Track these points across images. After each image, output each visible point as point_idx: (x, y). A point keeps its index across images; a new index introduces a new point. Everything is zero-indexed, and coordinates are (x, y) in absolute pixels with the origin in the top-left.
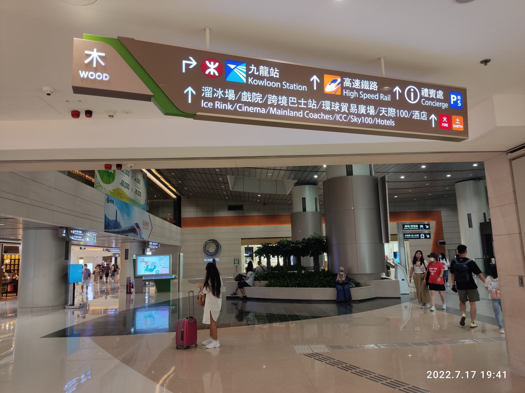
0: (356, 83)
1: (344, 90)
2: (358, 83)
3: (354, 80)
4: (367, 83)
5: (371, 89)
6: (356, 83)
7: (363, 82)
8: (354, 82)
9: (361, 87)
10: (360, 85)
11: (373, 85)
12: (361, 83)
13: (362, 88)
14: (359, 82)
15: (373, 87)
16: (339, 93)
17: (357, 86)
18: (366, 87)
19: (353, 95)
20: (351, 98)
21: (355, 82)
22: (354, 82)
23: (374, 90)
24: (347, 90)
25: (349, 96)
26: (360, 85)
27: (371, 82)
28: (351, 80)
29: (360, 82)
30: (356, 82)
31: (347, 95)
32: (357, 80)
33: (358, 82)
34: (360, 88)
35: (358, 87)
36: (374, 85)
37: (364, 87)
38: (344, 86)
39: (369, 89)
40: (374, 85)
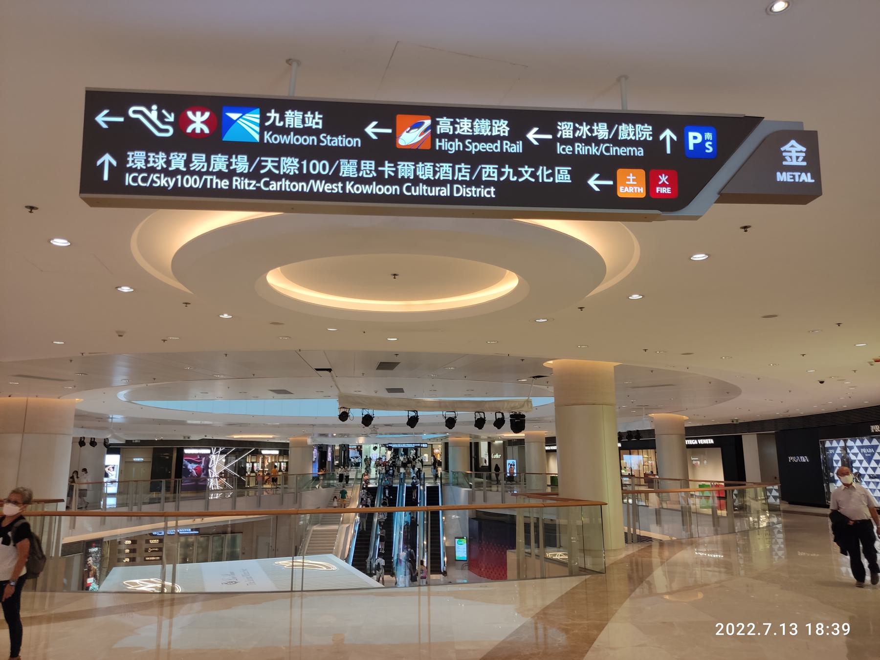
0: (463, 125)
2: (468, 125)
3: (458, 120)
6: (463, 125)
9: (473, 132)
10: (472, 128)
11: (498, 127)
12: (474, 124)
13: (475, 134)
14: (470, 124)
17: (466, 131)
18: (483, 131)
21: (462, 123)
22: (459, 123)
26: (472, 128)
28: (452, 120)
29: (472, 123)
30: (463, 123)
34: (471, 134)
35: (468, 131)
36: (502, 126)
37: (480, 132)
39: (489, 134)
40: (502, 126)
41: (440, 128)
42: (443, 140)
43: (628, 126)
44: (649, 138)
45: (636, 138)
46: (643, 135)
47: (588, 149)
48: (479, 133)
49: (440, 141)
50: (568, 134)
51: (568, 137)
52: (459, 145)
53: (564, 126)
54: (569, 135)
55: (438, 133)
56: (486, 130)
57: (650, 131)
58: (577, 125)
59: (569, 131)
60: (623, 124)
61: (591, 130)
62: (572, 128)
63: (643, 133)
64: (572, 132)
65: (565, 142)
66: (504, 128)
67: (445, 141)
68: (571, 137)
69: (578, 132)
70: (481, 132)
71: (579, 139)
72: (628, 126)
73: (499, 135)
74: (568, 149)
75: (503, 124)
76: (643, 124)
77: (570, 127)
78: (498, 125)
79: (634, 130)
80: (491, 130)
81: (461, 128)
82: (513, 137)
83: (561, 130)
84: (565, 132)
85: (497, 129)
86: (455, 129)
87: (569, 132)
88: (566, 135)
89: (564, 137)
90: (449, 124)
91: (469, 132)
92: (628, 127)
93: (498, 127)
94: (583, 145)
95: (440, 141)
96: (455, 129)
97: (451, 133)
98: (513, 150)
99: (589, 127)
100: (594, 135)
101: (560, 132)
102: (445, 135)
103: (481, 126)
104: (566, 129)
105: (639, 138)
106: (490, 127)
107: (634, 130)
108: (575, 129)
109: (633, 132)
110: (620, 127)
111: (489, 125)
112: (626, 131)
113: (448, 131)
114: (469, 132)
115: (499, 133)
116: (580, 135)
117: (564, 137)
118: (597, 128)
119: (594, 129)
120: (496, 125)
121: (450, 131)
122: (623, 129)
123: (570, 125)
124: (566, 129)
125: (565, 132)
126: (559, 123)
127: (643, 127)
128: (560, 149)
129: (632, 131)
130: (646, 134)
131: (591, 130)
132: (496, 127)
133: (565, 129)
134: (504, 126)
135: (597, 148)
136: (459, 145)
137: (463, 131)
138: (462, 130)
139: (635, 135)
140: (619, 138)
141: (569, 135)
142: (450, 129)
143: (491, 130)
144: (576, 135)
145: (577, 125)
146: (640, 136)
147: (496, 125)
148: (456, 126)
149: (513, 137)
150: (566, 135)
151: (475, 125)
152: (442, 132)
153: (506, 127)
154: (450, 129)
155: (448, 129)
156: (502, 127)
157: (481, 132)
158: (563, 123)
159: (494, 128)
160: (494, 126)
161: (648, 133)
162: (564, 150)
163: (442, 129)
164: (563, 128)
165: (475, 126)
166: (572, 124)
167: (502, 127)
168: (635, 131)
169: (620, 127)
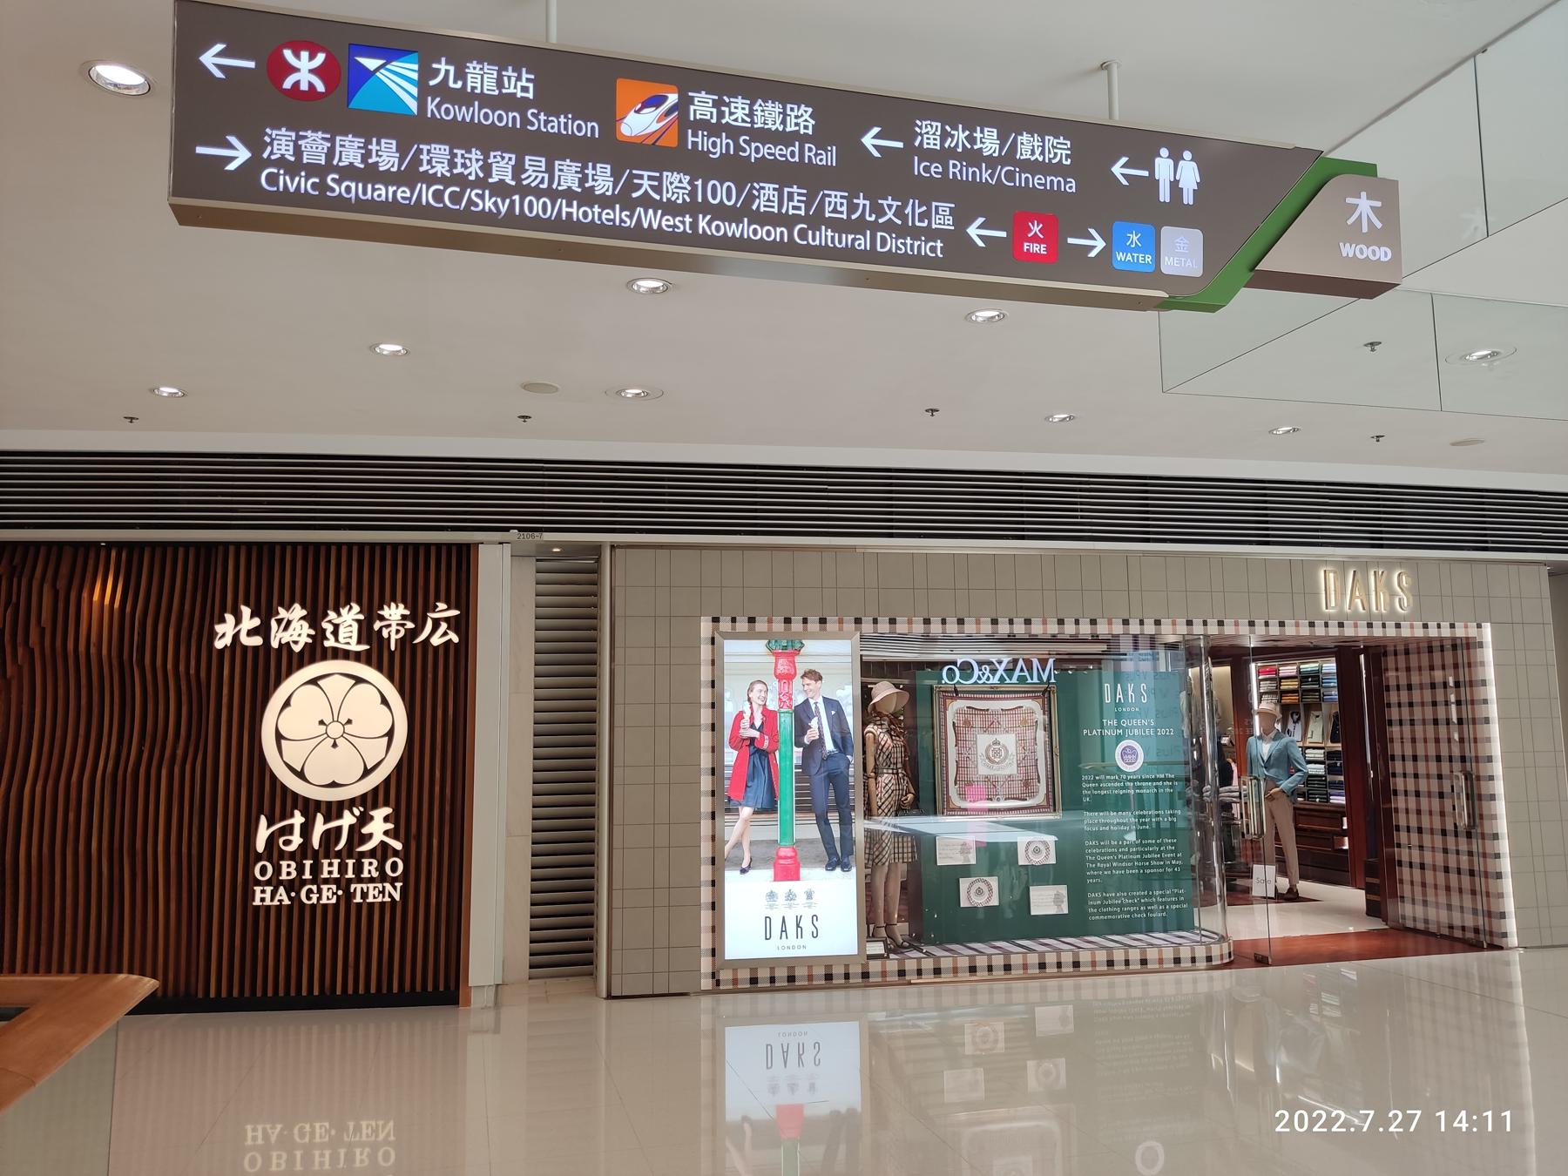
0: (736, 108)
1: (690, 131)
2: (743, 109)
4: (777, 110)
5: (788, 129)
6: (736, 108)
7: (760, 105)
8: (728, 105)
9: (752, 122)
10: (751, 114)
12: (755, 108)
13: (756, 126)
14: (747, 107)
15: (797, 124)
16: (671, 141)
17: (740, 120)
18: (770, 122)
19: (719, 147)
20: (711, 156)
21: (733, 105)
22: (728, 105)
23: (802, 131)
24: (700, 132)
25: (706, 150)
26: (751, 114)
27: (789, 106)
31: (700, 149)
32: (740, 99)
33: (744, 106)
34: (749, 125)
35: (743, 121)
38: (692, 119)
39: (781, 129)
41: (695, 111)
42: (700, 132)
43: (1033, 136)
44: (1066, 160)
45: (1044, 158)
46: (1056, 154)
47: (974, 173)
48: (762, 125)
49: (695, 135)
50: (932, 141)
51: (932, 146)
52: (728, 144)
53: (926, 127)
54: (935, 144)
55: (692, 119)
56: (775, 122)
57: (1068, 149)
58: (948, 128)
59: (935, 137)
60: (1025, 133)
61: (971, 139)
62: (939, 133)
63: (1055, 151)
64: (938, 138)
65: (928, 155)
66: (806, 121)
67: (703, 135)
68: (938, 147)
69: (950, 139)
70: (767, 124)
71: (951, 153)
72: (1033, 136)
73: (798, 131)
74: (936, 169)
75: (804, 114)
76: (1056, 137)
77: (936, 130)
78: (796, 113)
79: (1041, 144)
80: (784, 122)
81: (731, 114)
82: (820, 139)
83: (921, 134)
84: (928, 139)
85: (794, 121)
86: (721, 115)
87: (935, 139)
88: (928, 144)
89: (925, 146)
90: (710, 105)
91: (746, 122)
92: (1032, 139)
93: (797, 117)
94: (964, 164)
95: (695, 135)
96: (721, 115)
97: (714, 121)
98: (821, 160)
99: (967, 133)
100: (976, 147)
101: (920, 138)
102: (702, 125)
103: (766, 112)
104: (929, 134)
105: (1050, 159)
106: (781, 116)
107: (1041, 144)
108: (945, 136)
109: (1040, 149)
110: (1019, 138)
111: (780, 113)
112: (1028, 146)
113: (708, 117)
114: (746, 122)
115: (797, 128)
116: (952, 145)
117: (925, 146)
118: (982, 136)
119: (976, 137)
120: (793, 114)
121: (712, 118)
122: (1025, 142)
123: (937, 127)
124: (929, 134)
125: (928, 139)
126: (918, 122)
127: (1056, 141)
128: (918, 167)
129: (1038, 146)
130: (1061, 154)
131: (971, 139)
132: (793, 117)
133: (927, 133)
134: (806, 116)
135: (990, 171)
136: (728, 144)
137: (736, 120)
138: (733, 117)
139: (1042, 153)
140: (1018, 157)
141: (935, 144)
142: (712, 113)
143: (784, 122)
144: (946, 146)
145: (948, 128)
146: (1052, 156)
147: (793, 114)
148: (723, 108)
149: (820, 139)
150: (928, 144)
151: (757, 110)
152: (698, 117)
153: (809, 119)
154: (712, 113)
155: (709, 114)
156: (803, 119)
157: (767, 124)
158: (924, 123)
159: (788, 118)
160: (789, 115)
161: (1064, 152)
162: (927, 169)
163: (698, 112)
164: (924, 131)
165: (755, 113)
166: (939, 124)
167: (802, 118)
168: (1043, 147)
169: (1019, 138)
